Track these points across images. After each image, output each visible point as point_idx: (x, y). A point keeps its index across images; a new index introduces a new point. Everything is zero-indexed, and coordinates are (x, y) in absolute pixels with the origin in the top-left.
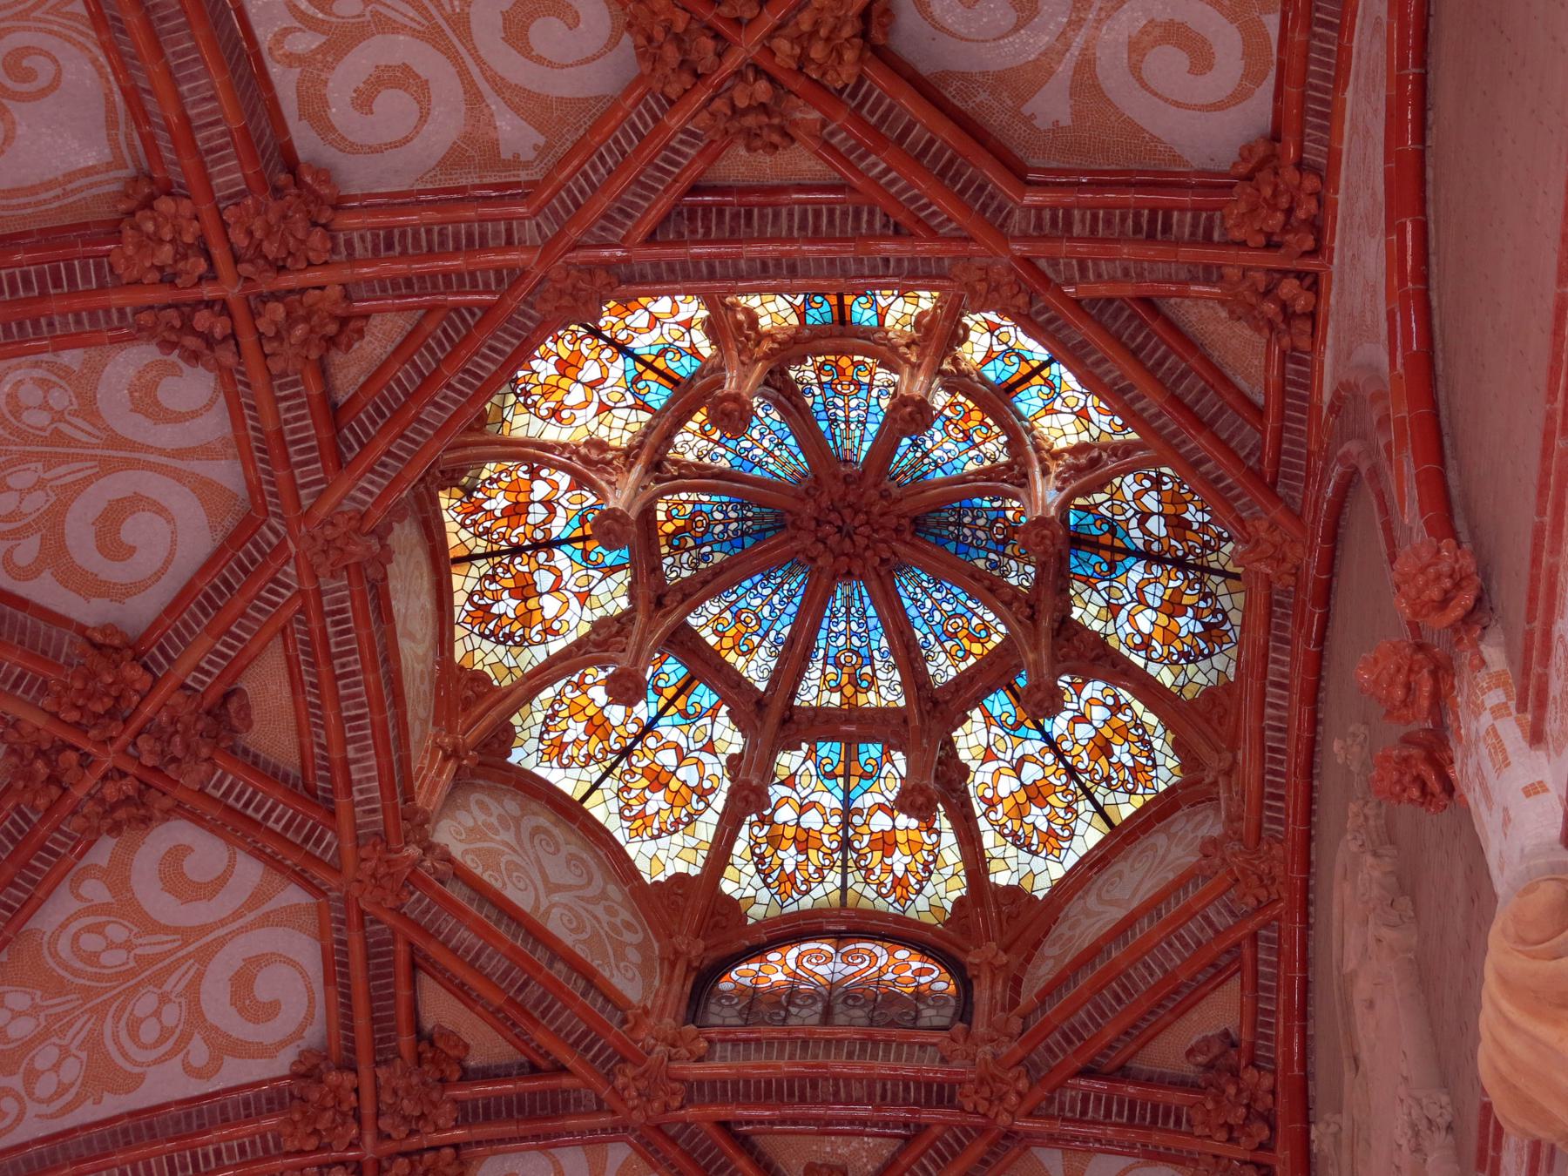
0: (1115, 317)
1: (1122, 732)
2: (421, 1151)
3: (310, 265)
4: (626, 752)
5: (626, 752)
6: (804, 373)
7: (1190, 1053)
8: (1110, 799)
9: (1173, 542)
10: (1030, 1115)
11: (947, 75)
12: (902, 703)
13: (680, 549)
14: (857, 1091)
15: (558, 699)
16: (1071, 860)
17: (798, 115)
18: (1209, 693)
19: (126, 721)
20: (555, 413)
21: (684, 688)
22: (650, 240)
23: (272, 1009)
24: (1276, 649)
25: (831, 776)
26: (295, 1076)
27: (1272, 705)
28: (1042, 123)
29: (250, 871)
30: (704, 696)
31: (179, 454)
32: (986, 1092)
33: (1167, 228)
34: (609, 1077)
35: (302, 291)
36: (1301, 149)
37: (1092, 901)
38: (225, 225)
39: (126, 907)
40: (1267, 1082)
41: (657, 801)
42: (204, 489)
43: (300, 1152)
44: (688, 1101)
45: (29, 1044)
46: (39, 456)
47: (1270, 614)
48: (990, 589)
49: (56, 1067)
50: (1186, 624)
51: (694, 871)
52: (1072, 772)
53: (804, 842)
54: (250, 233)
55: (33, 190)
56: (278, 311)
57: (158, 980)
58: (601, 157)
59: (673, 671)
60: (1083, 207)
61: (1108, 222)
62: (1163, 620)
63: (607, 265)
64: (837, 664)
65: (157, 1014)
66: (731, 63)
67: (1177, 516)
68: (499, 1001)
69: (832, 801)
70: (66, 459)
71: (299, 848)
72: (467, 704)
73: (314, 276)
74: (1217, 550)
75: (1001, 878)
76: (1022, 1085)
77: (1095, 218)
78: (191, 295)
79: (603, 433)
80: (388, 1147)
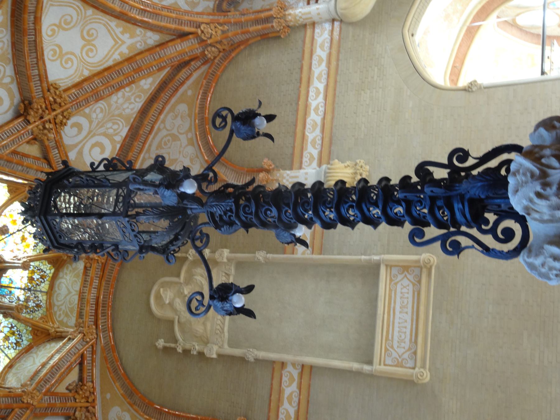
8: (9, 352)
9: (29, 284)
18: (41, 318)
24: (95, 280)
27: (93, 293)
32: (30, 396)
50: (31, 304)
58: (6, 133)
62: (25, 304)
66: (46, 118)
67: (31, 277)
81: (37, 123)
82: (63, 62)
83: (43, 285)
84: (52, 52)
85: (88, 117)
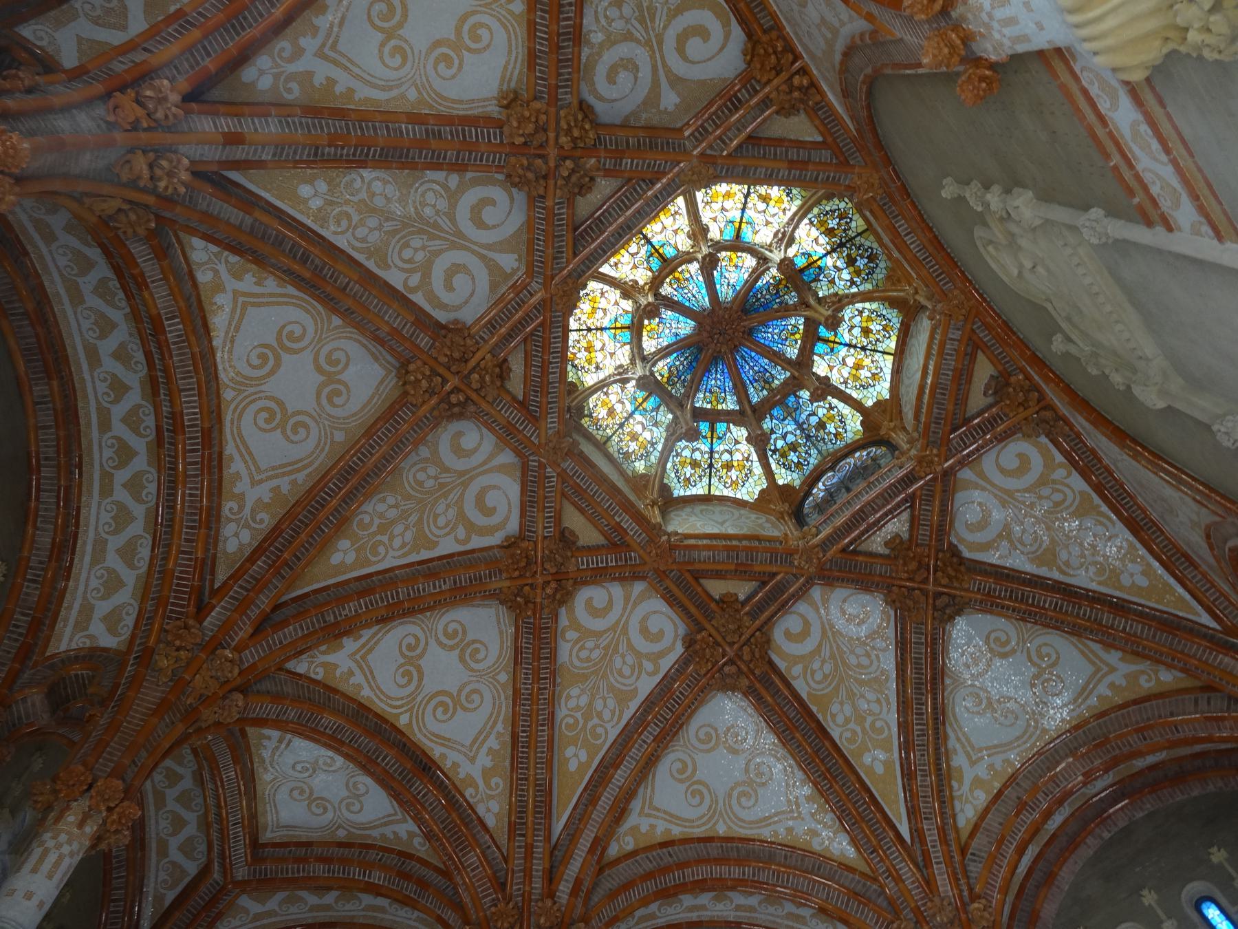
0: (747, 151)
1: (869, 319)
2: (749, 640)
3: (474, 353)
4: (711, 466)
5: (711, 466)
6: (666, 290)
7: (985, 394)
10: (946, 461)
11: (627, 118)
12: (788, 374)
13: (674, 384)
14: (880, 502)
15: (674, 465)
16: (888, 377)
17: (588, 166)
18: (888, 278)
19: (536, 563)
20: (597, 368)
21: (713, 430)
22: (575, 255)
23: (661, 633)
25: (784, 419)
26: (687, 648)
28: (671, 108)
29: (616, 590)
30: (721, 427)
31: (485, 463)
33: (739, 101)
34: (791, 563)
35: (478, 364)
36: (761, 26)
37: (906, 381)
38: (436, 359)
39: (587, 633)
40: (1021, 377)
41: (734, 474)
42: (501, 469)
43: (708, 672)
44: (825, 552)
45: (590, 704)
46: (440, 497)
47: (884, 211)
48: (786, 311)
49: (605, 706)
50: (861, 263)
51: (765, 486)
52: (863, 349)
53: (793, 447)
54: (446, 355)
55: (369, 402)
56: (476, 376)
57: (616, 651)
59: (704, 427)
60: (706, 120)
61: (718, 118)
62: (852, 269)
63: (570, 275)
64: (756, 381)
65: (624, 663)
66: (552, 164)
68: (733, 567)
69: (791, 427)
70: (449, 491)
71: (626, 565)
72: (646, 487)
73: (479, 355)
74: (850, 228)
75: (869, 403)
76: (935, 451)
77: (713, 121)
78: (443, 393)
79: (618, 363)
80: (736, 646)
81: (551, 187)
82: (473, 46)
83: (853, 224)
84: (442, 66)
85: (611, 41)
